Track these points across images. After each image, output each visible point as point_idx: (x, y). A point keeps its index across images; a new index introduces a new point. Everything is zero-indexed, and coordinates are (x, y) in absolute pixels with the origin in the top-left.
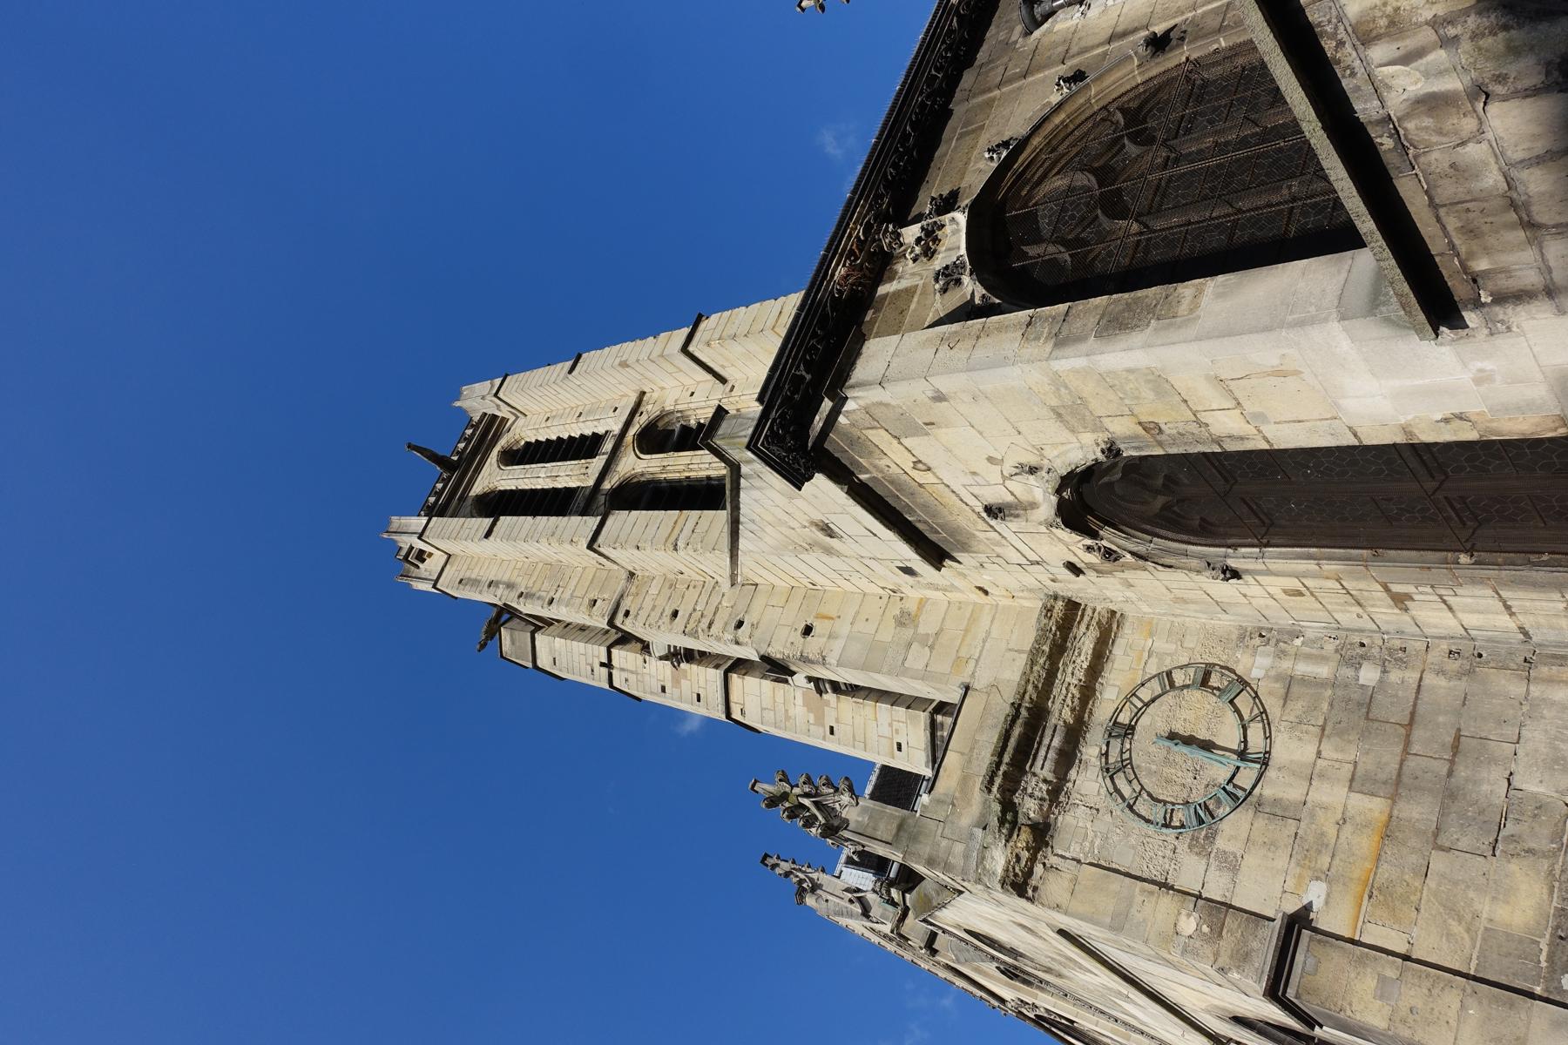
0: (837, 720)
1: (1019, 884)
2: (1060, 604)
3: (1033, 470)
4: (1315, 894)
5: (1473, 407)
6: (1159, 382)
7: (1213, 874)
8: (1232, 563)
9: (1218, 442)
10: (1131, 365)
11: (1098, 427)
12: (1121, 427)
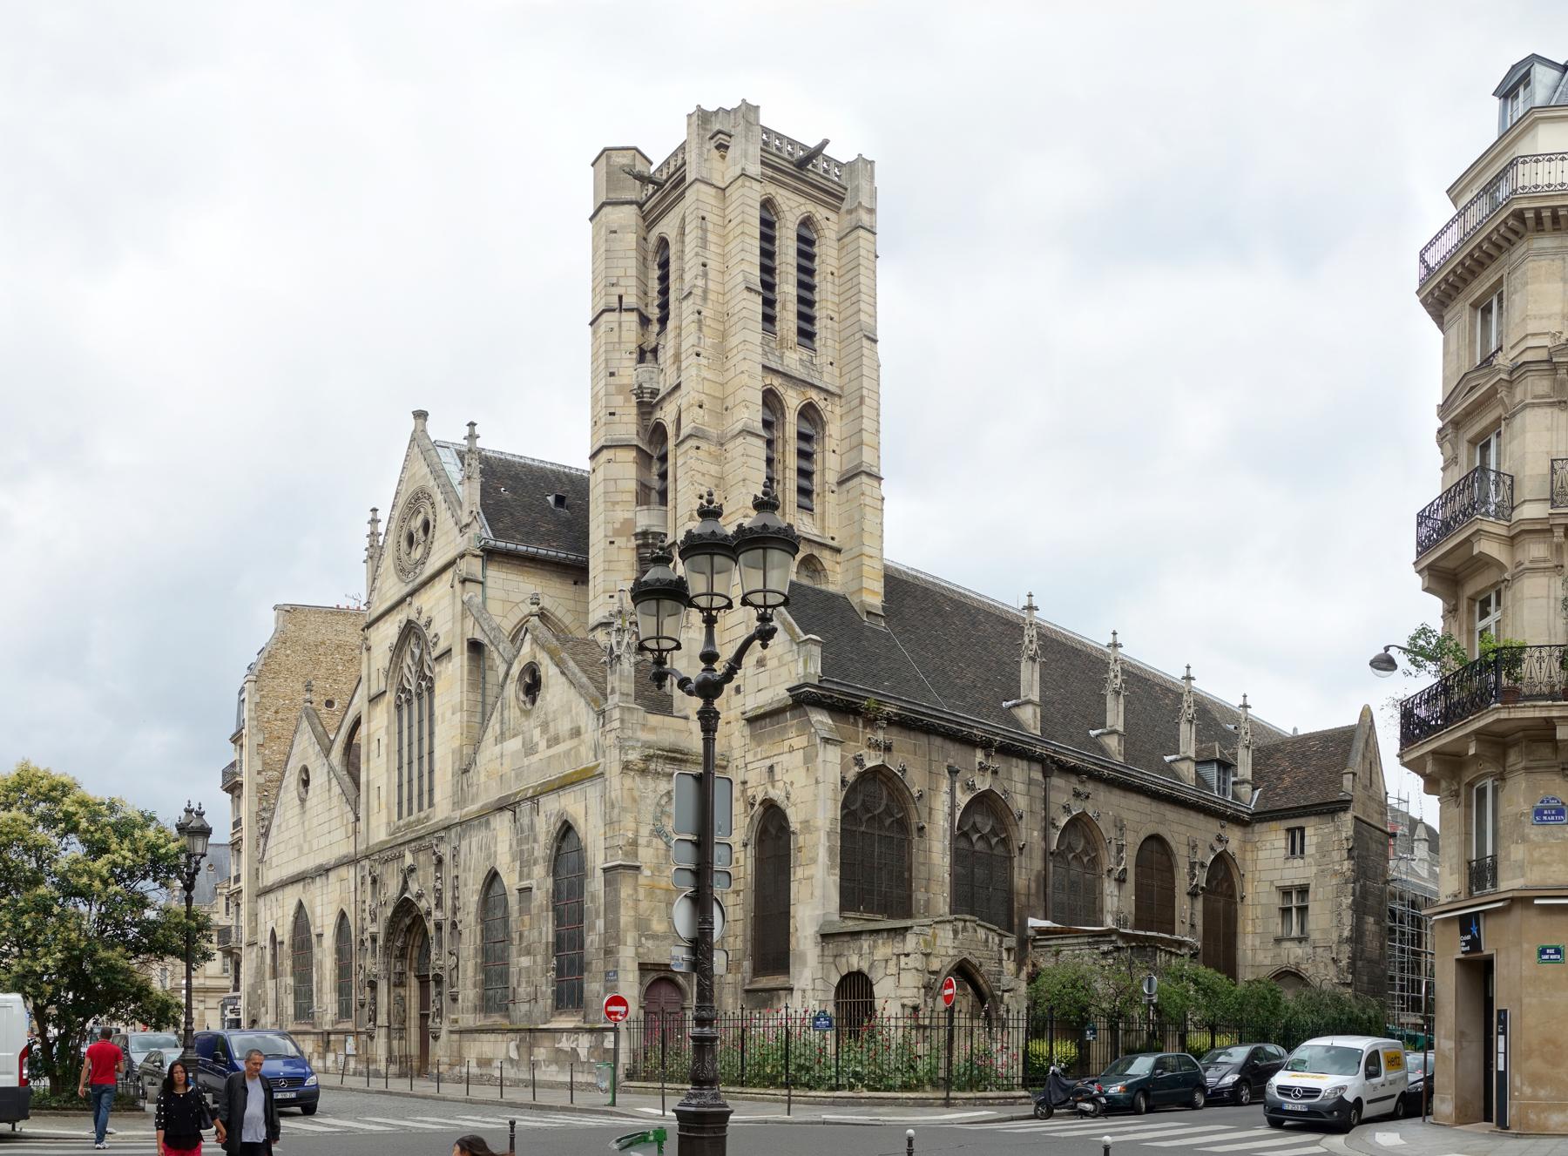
0: (619, 548)
1: (626, 767)
2: (725, 763)
3: (788, 798)
4: (647, 872)
5: (799, 934)
6: (814, 861)
7: (646, 839)
8: (749, 847)
9: (794, 867)
10: (820, 855)
11: (801, 833)
12: (801, 838)
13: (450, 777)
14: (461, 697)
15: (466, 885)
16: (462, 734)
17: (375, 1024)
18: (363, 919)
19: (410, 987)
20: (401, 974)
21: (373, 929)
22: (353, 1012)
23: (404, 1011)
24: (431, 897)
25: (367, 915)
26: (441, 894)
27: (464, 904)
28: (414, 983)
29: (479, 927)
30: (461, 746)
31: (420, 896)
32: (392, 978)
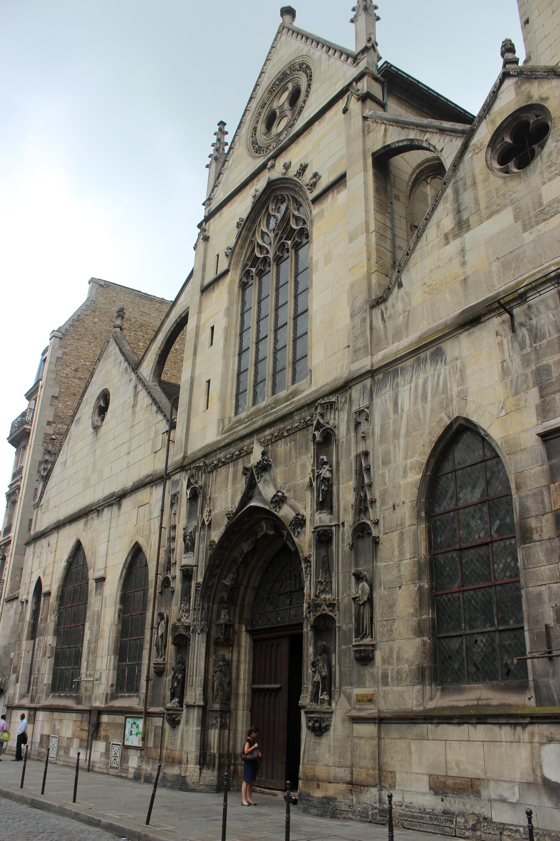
13: (348, 320)
14: (367, 217)
15: (386, 463)
16: (369, 260)
17: (181, 703)
18: (171, 551)
19: (239, 646)
20: (229, 626)
21: (188, 560)
22: (143, 683)
23: (230, 683)
24: (302, 500)
25: (179, 544)
26: (330, 486)
27: (384, 493)
28: (245, 640)
29: (423, 526)
30: (369, 274)
31: (279, 500)
32: (213, 633)
